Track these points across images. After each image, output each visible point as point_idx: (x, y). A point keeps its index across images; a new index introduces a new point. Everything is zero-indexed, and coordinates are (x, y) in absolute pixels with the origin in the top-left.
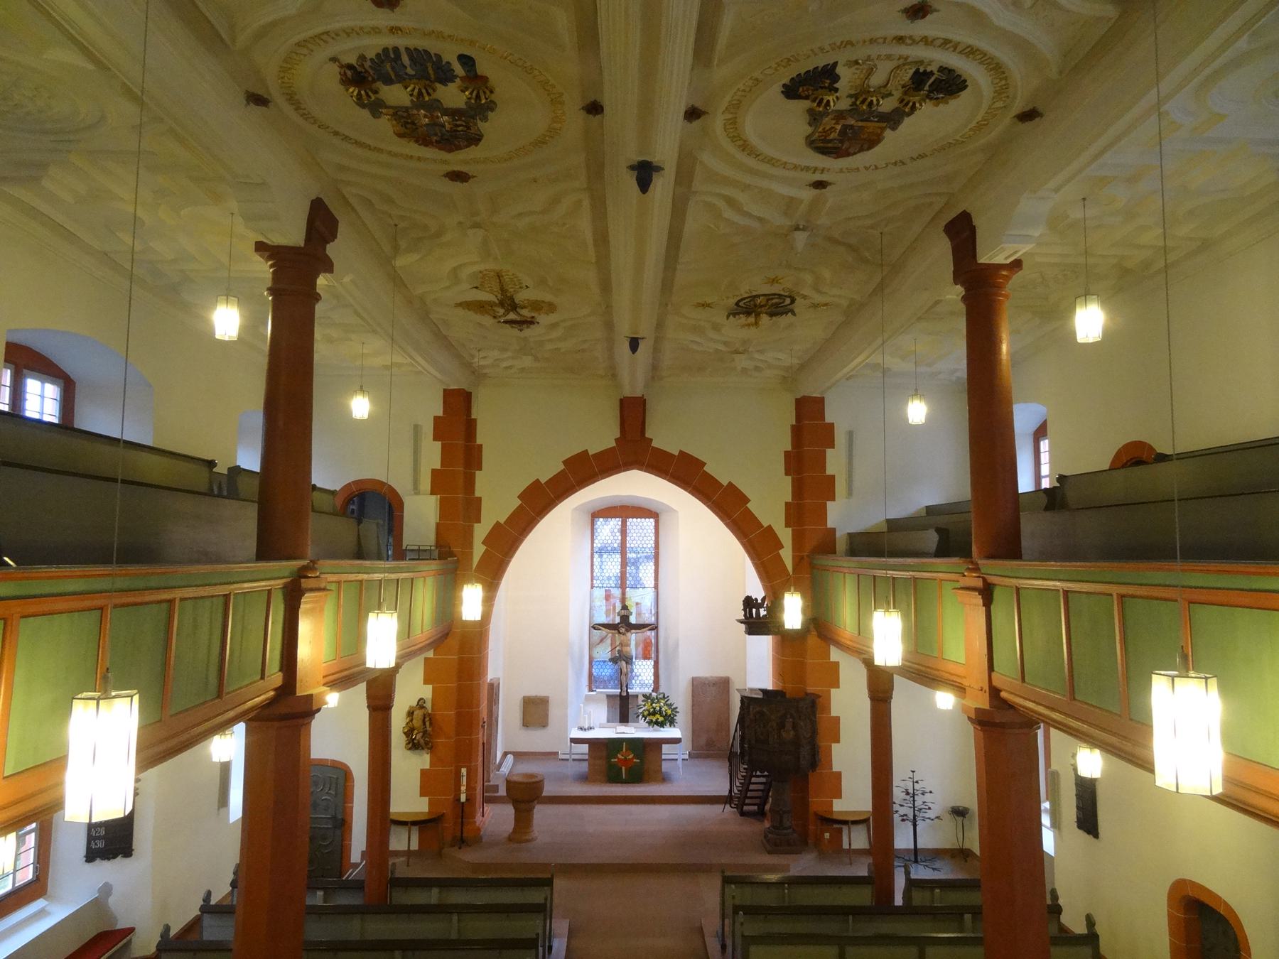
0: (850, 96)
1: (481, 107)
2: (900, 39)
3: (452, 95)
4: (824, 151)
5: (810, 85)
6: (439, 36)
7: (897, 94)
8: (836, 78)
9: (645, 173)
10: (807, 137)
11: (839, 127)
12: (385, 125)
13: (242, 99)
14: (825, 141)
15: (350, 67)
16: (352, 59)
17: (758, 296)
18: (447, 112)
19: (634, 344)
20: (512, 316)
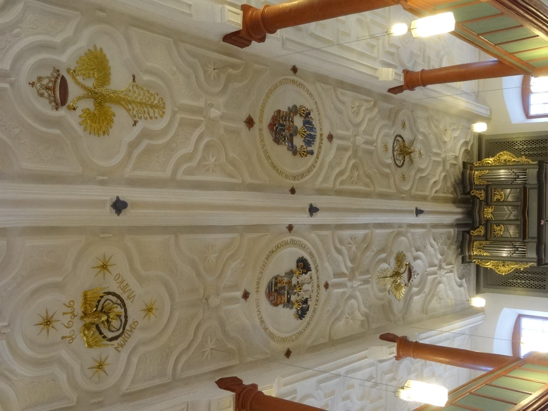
0: (298, 282)
1: (294, 151)
2: (318, 286)
3: (298, 141)
4: (270, 287)
5: (303, 266)
6: (320, 147)
7: (298, 298)
8: (306, 273)
9: (313, 210)
10: (279, 276)
11: (284, 285)
12: (284, 109)
13: (298, 66)
14: (276, 284)
15: (309, 114)
16: (312, 115)
17: (124, 305)
18: (292, 136)
19: (119, 206)
20: (74, 91)
